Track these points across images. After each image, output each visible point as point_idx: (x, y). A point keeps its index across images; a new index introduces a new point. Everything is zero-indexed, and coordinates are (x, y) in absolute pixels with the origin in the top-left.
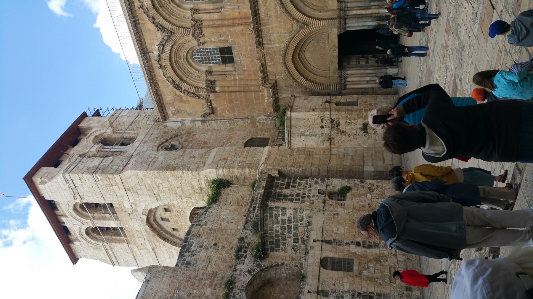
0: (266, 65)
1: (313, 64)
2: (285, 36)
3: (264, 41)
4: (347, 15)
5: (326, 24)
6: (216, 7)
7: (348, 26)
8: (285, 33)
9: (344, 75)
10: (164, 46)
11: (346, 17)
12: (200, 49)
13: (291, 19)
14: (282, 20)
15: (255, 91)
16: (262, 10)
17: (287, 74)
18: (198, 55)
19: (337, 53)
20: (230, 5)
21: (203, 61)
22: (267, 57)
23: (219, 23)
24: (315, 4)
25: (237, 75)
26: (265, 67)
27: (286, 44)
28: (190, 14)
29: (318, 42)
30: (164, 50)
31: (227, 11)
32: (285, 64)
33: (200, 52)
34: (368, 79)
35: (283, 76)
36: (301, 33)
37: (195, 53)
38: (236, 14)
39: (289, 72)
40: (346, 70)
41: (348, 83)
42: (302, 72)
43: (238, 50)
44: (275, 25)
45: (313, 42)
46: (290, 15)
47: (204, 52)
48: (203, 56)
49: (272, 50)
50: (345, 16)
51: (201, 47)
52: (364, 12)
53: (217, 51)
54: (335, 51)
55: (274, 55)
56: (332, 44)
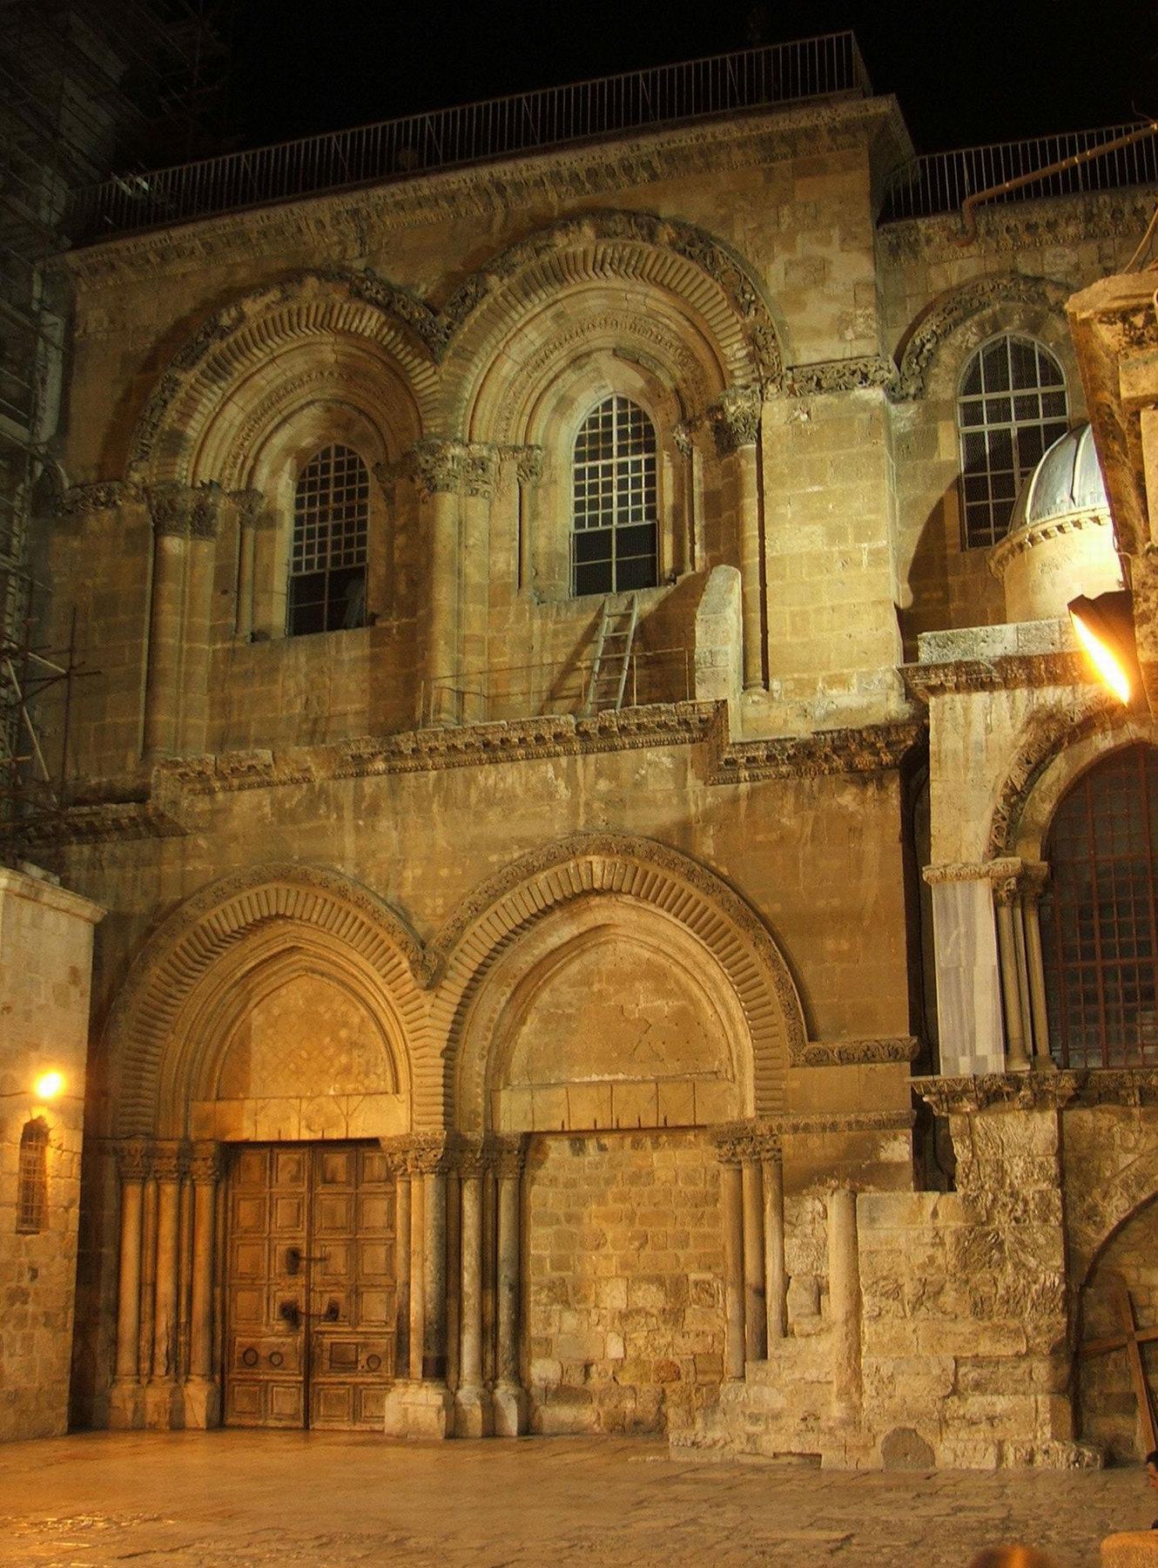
0: (260, 785)
3: (374, 779)
6: (543, 569)
7: (415, 1184)
10: (386, 307)
11: (454, 1175)
12: (364, 478)
15: (148, 727)
16: (511, 777)
18: (339, 466)
19: (294, 1137)
20: (543, 635)
21: (312, 486)
22: (298, 795)
23: (474, 575)
24: (525, 1029)
25: (228, 645)
26: (253, 779)
28: (521, 443)
29: (353, 1045)
30: (369, 309)
31: (520, 616)
33: (351, 480)
34: (166, 1287)
36: (395, 961)
37: (351, 452)
38: (502, 654)
41: (151, 1188)
43: (346, 656)
44: (441, 837)
46: (478, 910)
47: (351, 494)
48: (332, 490)
49: (328, 818)
51: (372, 484)
52: (470, 1259)
53: (349, 558)
54: (309, 1127)
55: (305, 826)
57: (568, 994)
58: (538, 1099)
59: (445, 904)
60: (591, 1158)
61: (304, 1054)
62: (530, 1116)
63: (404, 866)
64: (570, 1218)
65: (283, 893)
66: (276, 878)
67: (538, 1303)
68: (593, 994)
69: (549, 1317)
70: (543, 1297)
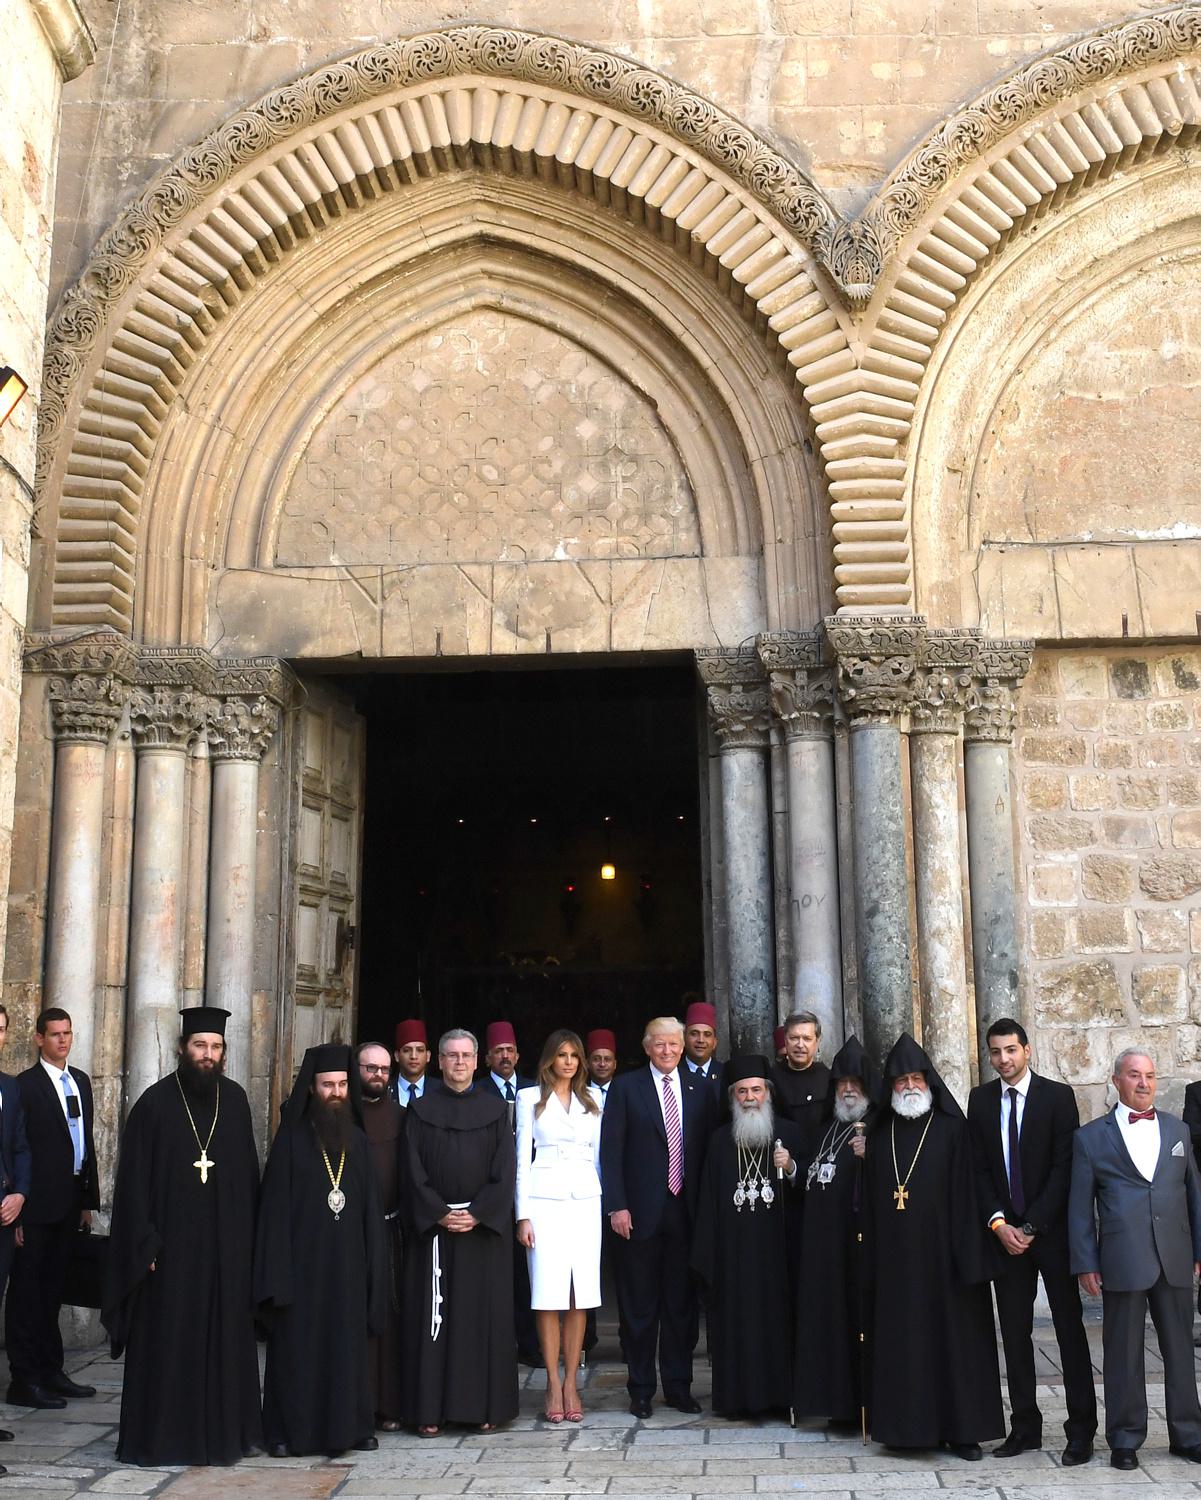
1: (372, 394)
2: (746, 84)
4: (913, 736)
5: (859, 505)
8: (776, 94)
9: (216, 729)
13: (943, 143)
14: (916, 70)
17: (320, 76)
19: (477, 646)
24: (1013, 430)
27: (662, 84)
29: (609, 454)
32: (432, 66)
35: (289, 47)
36: (774, 247)
39: (336, 97)
40: (263, 753)
41: (124, 760)
42: (304, 260)
45: (616, 398)
50: (915, 719)
52: (947, 913)
54: (512, 626)
56: (583, 590)
57: (1104, 361)
58: (1063, 568)
59: (889, 134)
60: (1158, 704)
61: (492, 474)
62: (1049, 607)
63: (785, 57)
64: (1116, 829)
65: (488, 100)
66: (477, 66)
67: (1054, 1013)
68: (1163, 362)
69: (1084, 1046)
70: (1065, 1000)
